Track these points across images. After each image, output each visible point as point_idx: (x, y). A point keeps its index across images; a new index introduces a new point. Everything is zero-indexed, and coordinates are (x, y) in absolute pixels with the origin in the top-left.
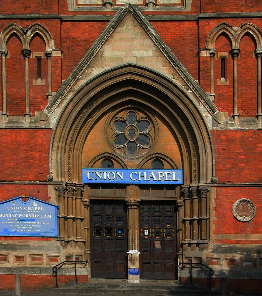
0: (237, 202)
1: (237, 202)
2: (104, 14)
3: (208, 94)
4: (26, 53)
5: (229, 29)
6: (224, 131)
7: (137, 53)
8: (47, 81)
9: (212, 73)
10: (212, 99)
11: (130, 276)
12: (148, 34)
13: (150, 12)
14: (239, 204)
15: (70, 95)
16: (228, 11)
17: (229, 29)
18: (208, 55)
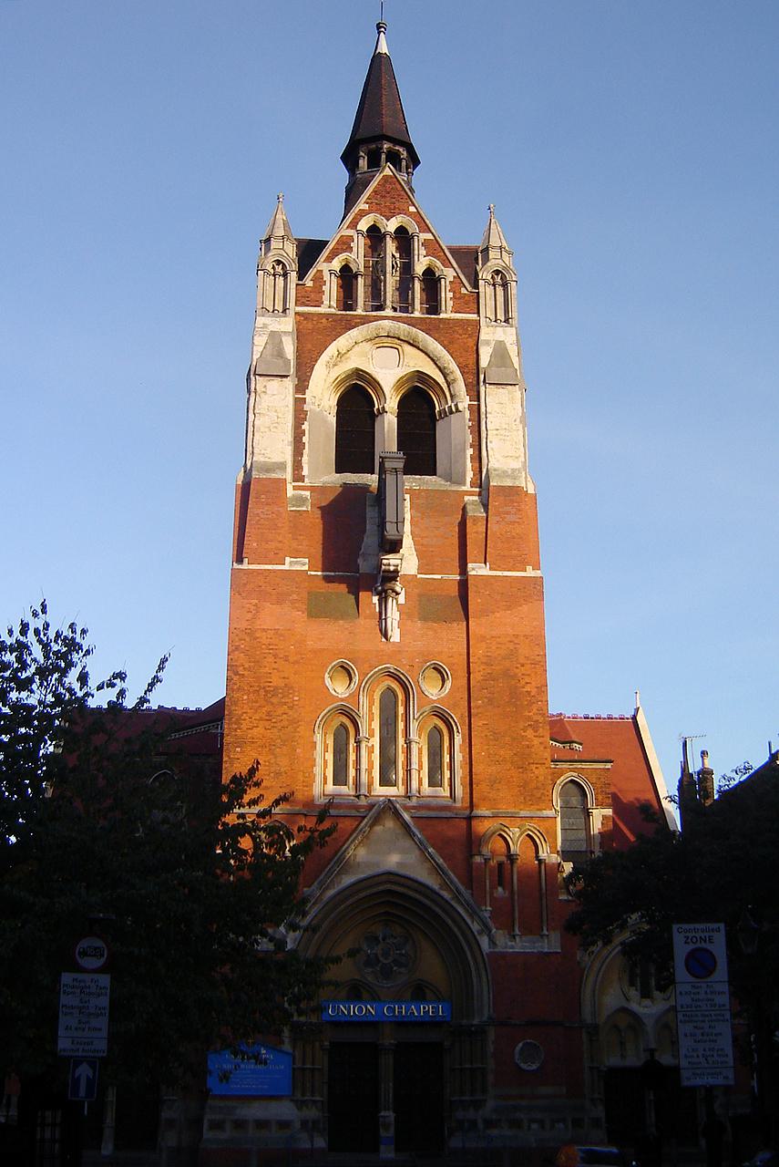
0: (521, 1045)
1: (521, 1045)
2: (357, 808)
3: (483, 908)
5: (506, 830)
6: (503, 955)
9: (488, 881)
10: (487, 915)
11: (382, 1148)
13: (414, 808)
14: (522, 1048)
16: (503, 808)
17: (506, 830)
18: (483, 861)
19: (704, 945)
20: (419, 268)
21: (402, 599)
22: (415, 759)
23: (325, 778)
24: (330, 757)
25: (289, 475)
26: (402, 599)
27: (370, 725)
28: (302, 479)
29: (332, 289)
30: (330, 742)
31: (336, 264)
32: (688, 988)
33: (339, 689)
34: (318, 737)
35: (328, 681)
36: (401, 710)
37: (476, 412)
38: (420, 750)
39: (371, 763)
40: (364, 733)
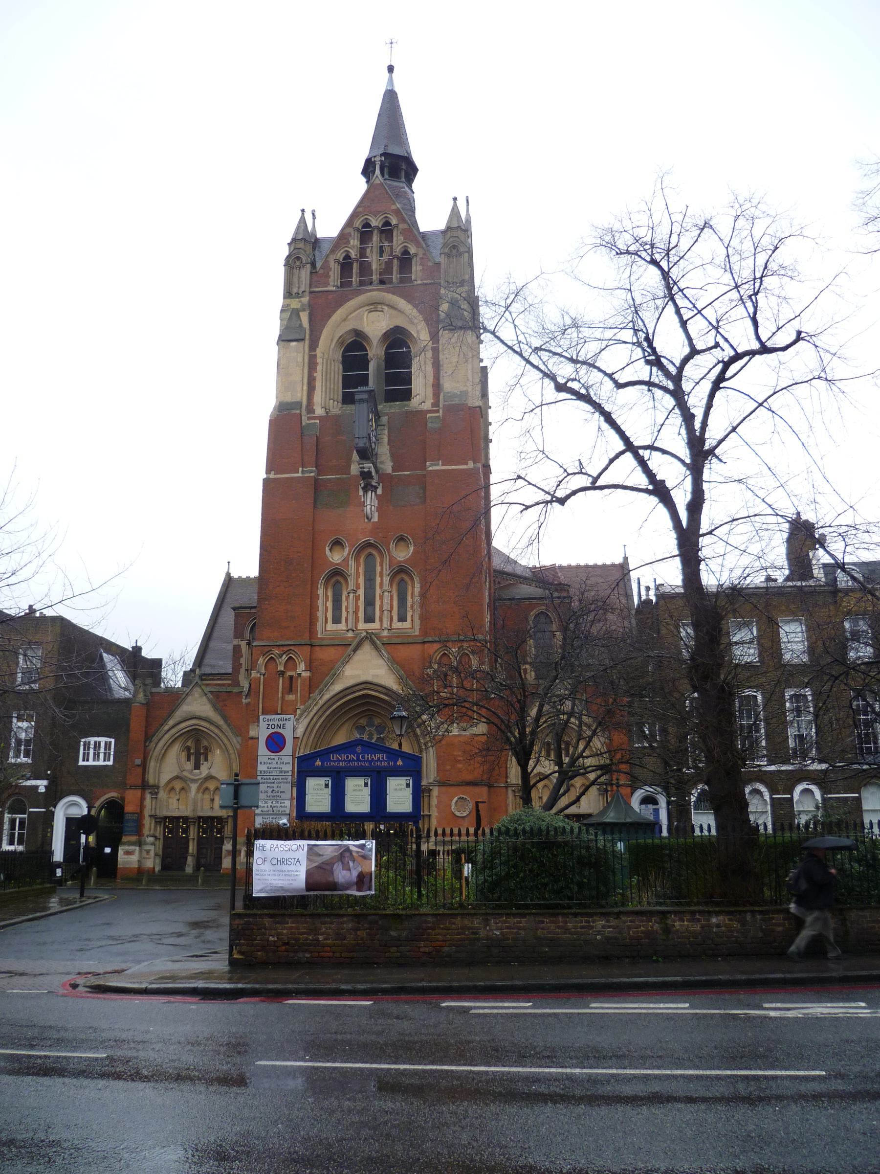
0: (456, 799)
4: (282, 673)
7: (373, 672)
8: (297, 696)
12: (382, 656)
13: (386, 637)
15: (316, 708)
19: (278, 730)
20: (398, 251)
21: (379, 491)
22: (385, 601)
23: (326, 619)
24: (330, 604)
25: (304, 412)
26: (379, 491)
27: (357, 581)
28: (313, 411)
29: (335, 271)
30: (330, 594)
31: (340, 255)
32: (265, 759)
33: (336, 557)
34: (321, 592)
35: (328, 552)
36: (378, 569)
37: (436, 351)
38: (392, 597)
39: (357, 608)
40: (351, 586)
